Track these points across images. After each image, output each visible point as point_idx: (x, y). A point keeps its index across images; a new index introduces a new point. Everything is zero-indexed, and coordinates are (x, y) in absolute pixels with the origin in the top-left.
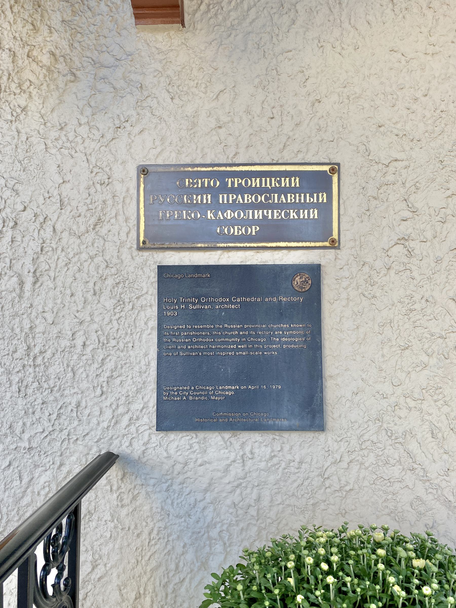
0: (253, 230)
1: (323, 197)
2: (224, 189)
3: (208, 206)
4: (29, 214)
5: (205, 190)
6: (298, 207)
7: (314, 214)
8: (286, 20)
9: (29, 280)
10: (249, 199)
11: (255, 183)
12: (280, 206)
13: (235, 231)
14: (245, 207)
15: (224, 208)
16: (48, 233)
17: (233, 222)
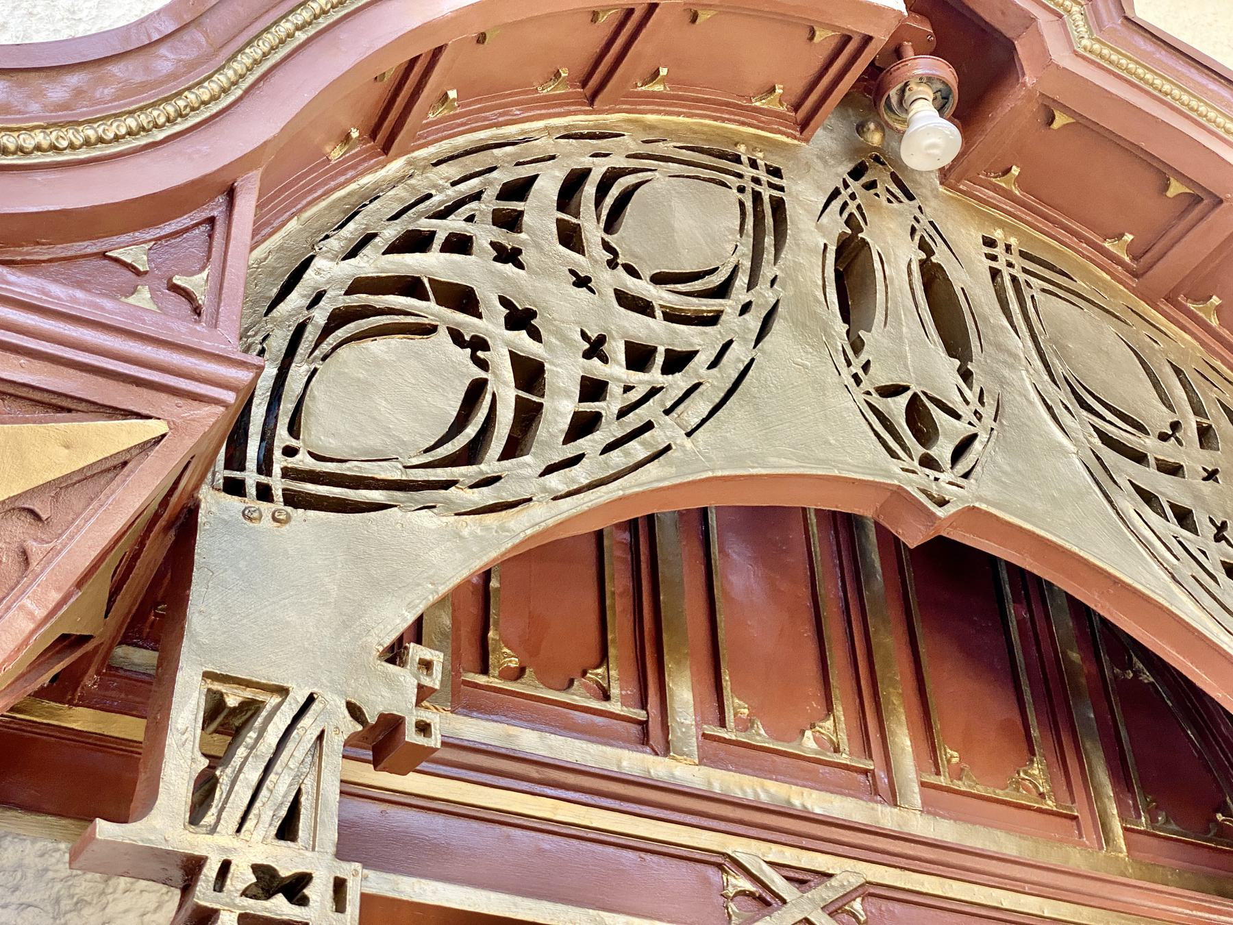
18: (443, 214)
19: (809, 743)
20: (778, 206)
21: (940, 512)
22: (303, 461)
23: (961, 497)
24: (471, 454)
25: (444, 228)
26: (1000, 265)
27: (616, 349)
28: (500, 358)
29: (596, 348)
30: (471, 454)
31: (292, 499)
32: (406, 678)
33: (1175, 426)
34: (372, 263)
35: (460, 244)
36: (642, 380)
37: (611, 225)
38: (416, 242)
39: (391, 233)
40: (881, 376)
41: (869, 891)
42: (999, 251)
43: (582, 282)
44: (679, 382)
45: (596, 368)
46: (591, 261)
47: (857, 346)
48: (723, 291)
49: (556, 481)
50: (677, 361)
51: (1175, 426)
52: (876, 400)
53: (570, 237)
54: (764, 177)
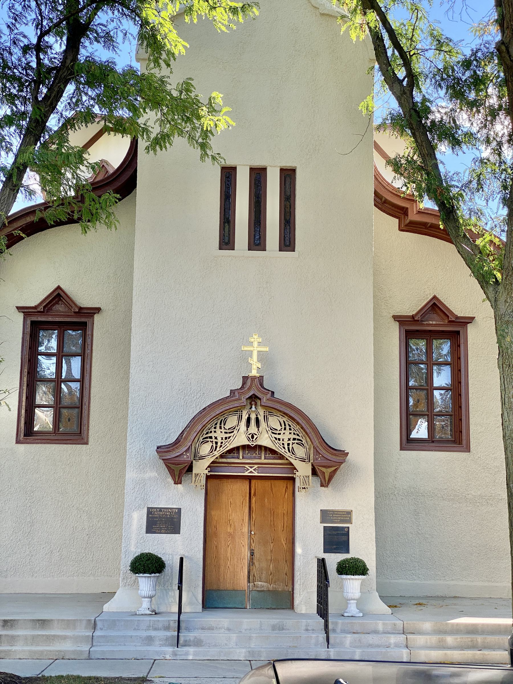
0: (339, 521)
1: (350, 516)
2: (334, 514)
3: (331, 517)
4: (302, 517)
5: (331, 514)
6: (346, 517)
7: (348, 518)
8: (344, 486)
9: (302, 528)
10: (338, 516)
11: (339, 513)
12: (343, 517)
13: (336, 521)
14: (337, 517)
15: (334, 517)
16: (306, 520)
17: (336, 519)
18: (209, 429)
19: (254, 454)
20: (242, 415)
21: (253, 446)
22: (200, 456)
23: (255, 444)
24: (212, 452)
25: (210, 431)
26: (265, 415)
27: (224, 439)
28: (214, 443)
29: (222, 439)
30: (212, 452)
31: (199, 459)
32: (207, 471)
33: (281, 429)
34: (205, 436)
35: (211, 432)
36: (226, 441)
37: (224, 425)
38: (207, 433)
39: (205, 433)
40: (249, 433)
41: (258, 467)
42: (266, 413)
43: (221, 432)
44: (229, 440)
45: (222, 441)
46: (223, 430)
47: (247, 430)
48: (234, 428)
49: (219, 452)
50: (229, 437)
51: (281, 429)
52: (248, 436)
53: (221, 428)
54: (240, 412)
